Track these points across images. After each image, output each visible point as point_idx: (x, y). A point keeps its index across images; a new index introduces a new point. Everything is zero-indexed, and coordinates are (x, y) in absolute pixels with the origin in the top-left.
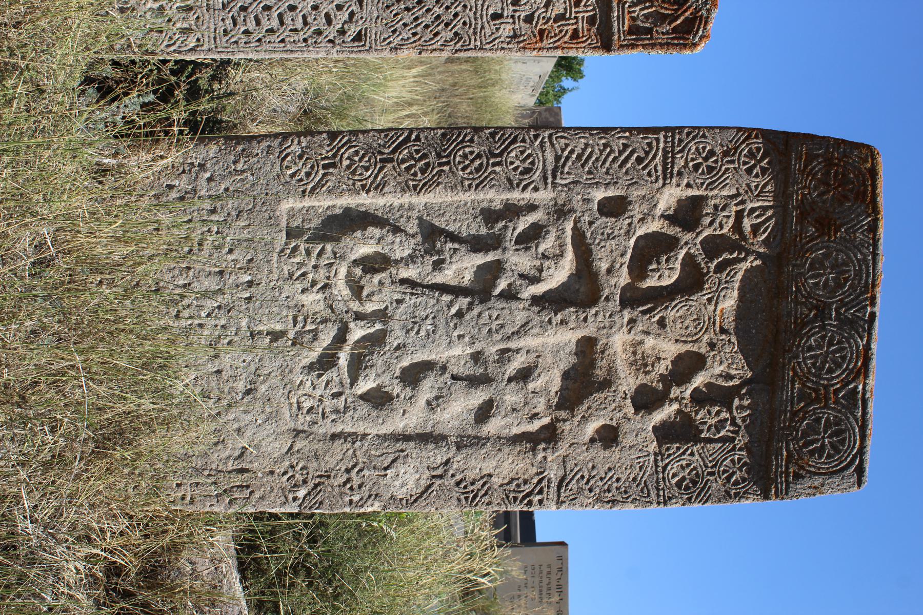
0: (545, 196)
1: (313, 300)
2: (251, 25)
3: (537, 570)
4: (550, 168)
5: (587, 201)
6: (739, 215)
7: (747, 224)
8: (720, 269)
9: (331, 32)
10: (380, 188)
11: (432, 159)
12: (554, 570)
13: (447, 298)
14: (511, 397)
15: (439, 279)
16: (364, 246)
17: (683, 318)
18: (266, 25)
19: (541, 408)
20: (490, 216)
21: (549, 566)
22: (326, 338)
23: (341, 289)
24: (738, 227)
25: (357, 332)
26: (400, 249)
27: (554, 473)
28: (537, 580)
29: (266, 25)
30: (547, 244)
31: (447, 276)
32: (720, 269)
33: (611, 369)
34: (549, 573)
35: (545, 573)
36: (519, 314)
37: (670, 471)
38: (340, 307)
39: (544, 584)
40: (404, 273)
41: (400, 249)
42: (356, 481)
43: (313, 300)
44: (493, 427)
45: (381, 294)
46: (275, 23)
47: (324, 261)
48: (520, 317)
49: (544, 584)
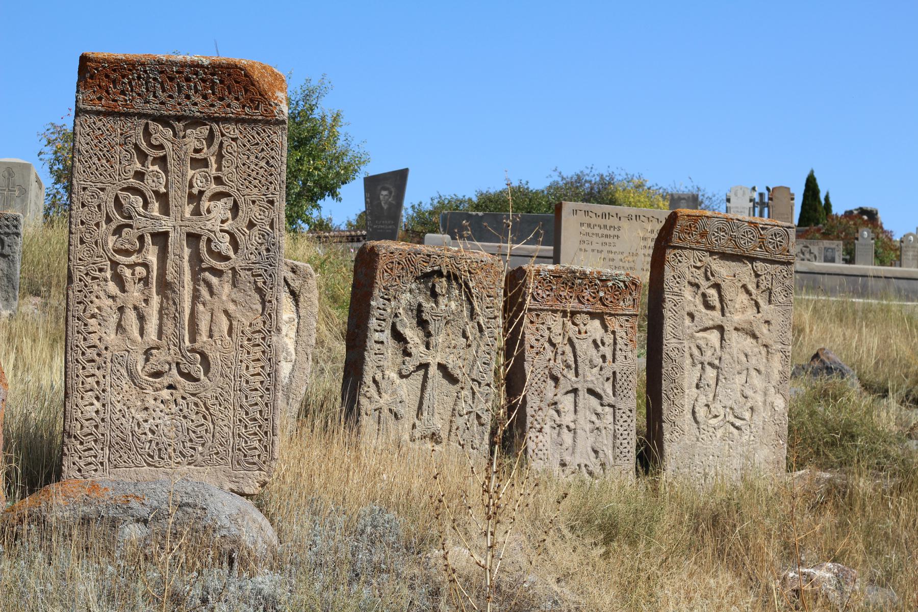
0: (686, 343)
1: (720, 433)
2: (626, 450)
3: (588, 238)
4: (677, 341)
5: (689, 328)
6: (695, 267)
7: (699, 264)
8: (713, 275)
9: (629, 420)
10: (683, 406)
11: (673, 386)
12: (586, 219)
13: (720, 383)
14: (753, 361)
15: (714, 386)
16: (701, 412)
17: (730, 292)
18: (626, 445)
19: (756, 350)
20: (694, 364)
21: (582, 224)
22: (732, 429)
23: (713, 422)
24: (698, 268)
25: (731, 418)
26: (703, 400)
27: (780, 346)
28: (595, 239)
29: (626, 445)
30: (702, 343)
31: (712, 382)
32: (713, 275)
33: (745, 322)
34: (589, 225)
35: (589, 230)
36: (726, 357)
37: (781, 301)
38: (722, 423)
39: (600, 232)
40: (711, 399)
41: (703, 400)
42: (778, 422)
43: (720, 433)
44: (762, 369)
45: (717, 408)
46: (626, 441)
47: (706, 428)
48: (727, 356)
49: (600, 232)
